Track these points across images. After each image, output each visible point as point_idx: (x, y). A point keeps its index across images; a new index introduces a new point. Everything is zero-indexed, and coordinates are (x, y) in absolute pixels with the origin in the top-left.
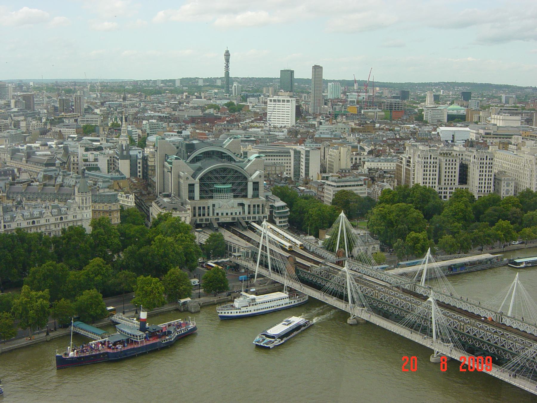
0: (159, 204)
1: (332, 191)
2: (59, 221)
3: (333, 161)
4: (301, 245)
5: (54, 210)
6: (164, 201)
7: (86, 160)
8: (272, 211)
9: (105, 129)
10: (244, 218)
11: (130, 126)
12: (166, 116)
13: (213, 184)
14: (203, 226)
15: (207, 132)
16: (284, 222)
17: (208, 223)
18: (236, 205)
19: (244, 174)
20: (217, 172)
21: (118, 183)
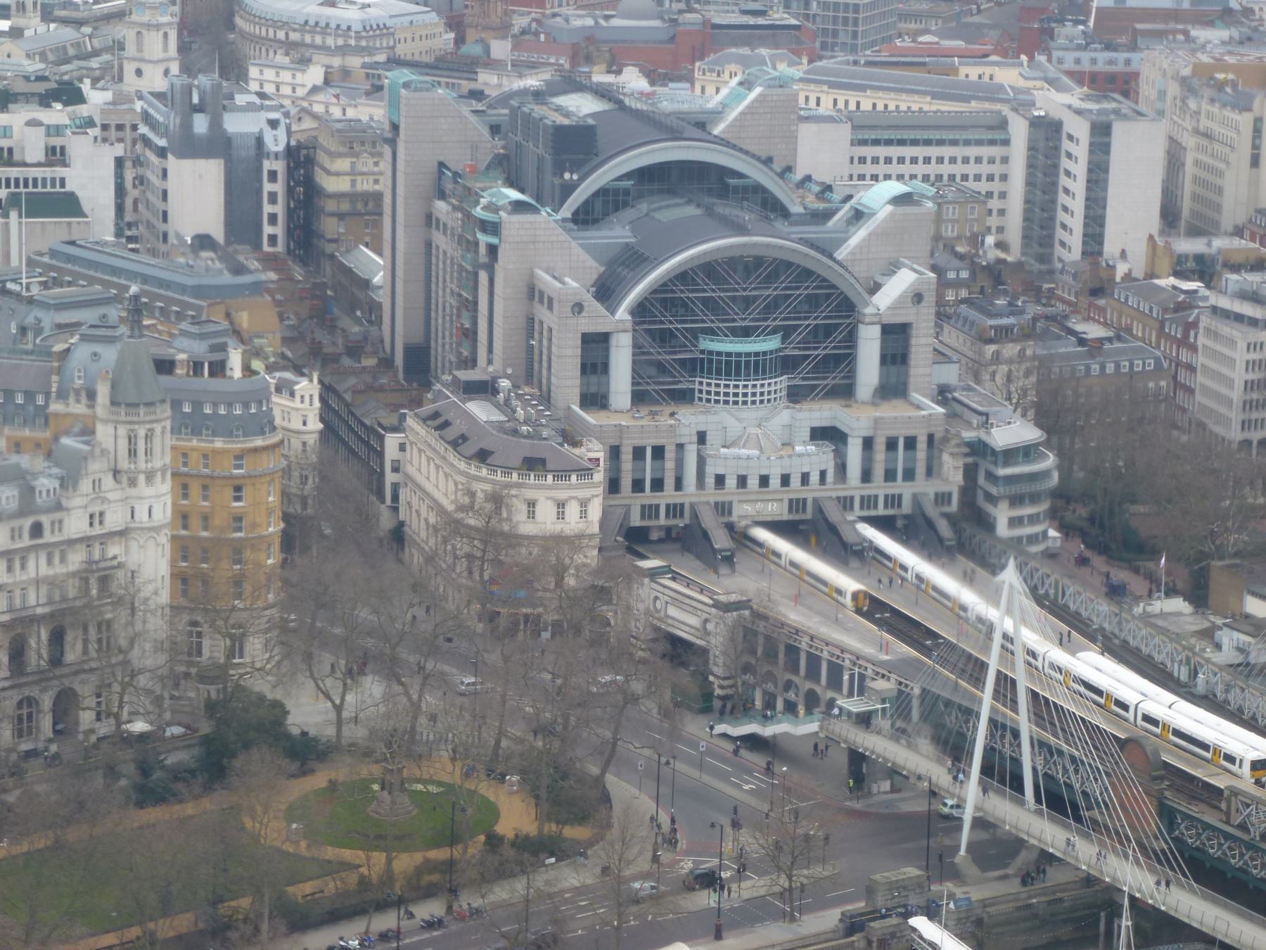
0: (451, 433)
1: (1242, 345)
2: (26, 541)
3: (1222, 166)
8: (976, 465)
10: (846, 503)
13: (695, 334)
14: (654, 536)
16: (1033, 519)
19: (843, 287)
21: (228, 315)
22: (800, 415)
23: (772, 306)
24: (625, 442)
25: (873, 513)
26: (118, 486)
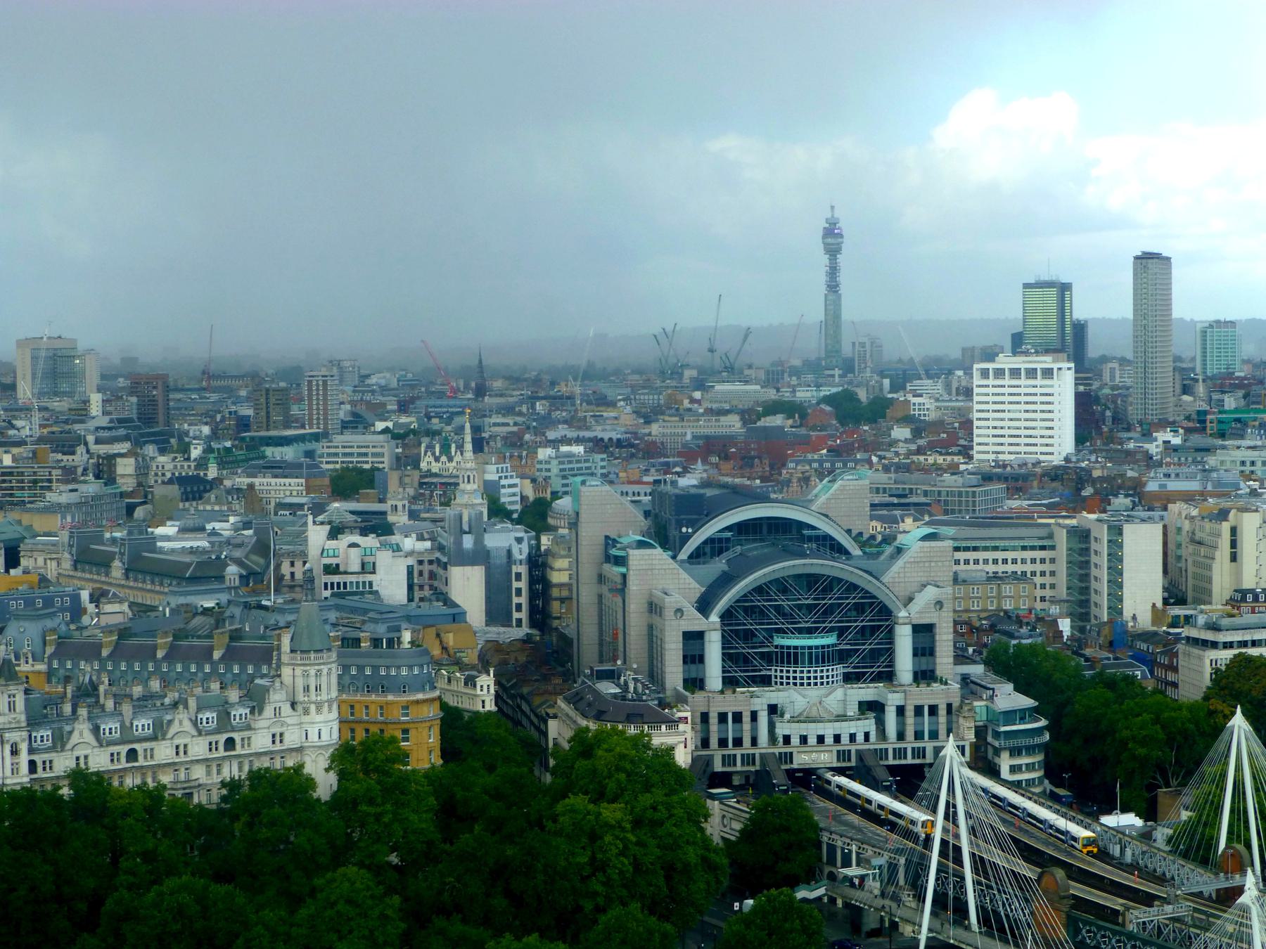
0: (582, 705)
2: (222, 752)
4: (1090, 842)
5: (205, 715)
6: (597, 693)
7: (331, 570)
9: (407, 480)
10: (883, 754)
11: (493, 468)
12: (619, 440)
13: (771, 633)
14: (736, 781)
15: (758, 481)
16: (1030, 768)
17: (752, 769)
18: (853, 710)
19: (881, 597)
20: (785, 591)
21: (438, 635)
22: (850, 692)
23: (829, 611)
24: (711, 709)
25: (903, 762)
26: (294, 713)
